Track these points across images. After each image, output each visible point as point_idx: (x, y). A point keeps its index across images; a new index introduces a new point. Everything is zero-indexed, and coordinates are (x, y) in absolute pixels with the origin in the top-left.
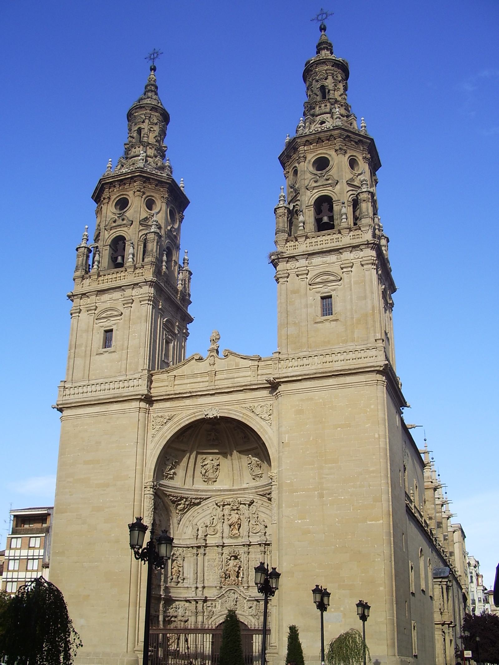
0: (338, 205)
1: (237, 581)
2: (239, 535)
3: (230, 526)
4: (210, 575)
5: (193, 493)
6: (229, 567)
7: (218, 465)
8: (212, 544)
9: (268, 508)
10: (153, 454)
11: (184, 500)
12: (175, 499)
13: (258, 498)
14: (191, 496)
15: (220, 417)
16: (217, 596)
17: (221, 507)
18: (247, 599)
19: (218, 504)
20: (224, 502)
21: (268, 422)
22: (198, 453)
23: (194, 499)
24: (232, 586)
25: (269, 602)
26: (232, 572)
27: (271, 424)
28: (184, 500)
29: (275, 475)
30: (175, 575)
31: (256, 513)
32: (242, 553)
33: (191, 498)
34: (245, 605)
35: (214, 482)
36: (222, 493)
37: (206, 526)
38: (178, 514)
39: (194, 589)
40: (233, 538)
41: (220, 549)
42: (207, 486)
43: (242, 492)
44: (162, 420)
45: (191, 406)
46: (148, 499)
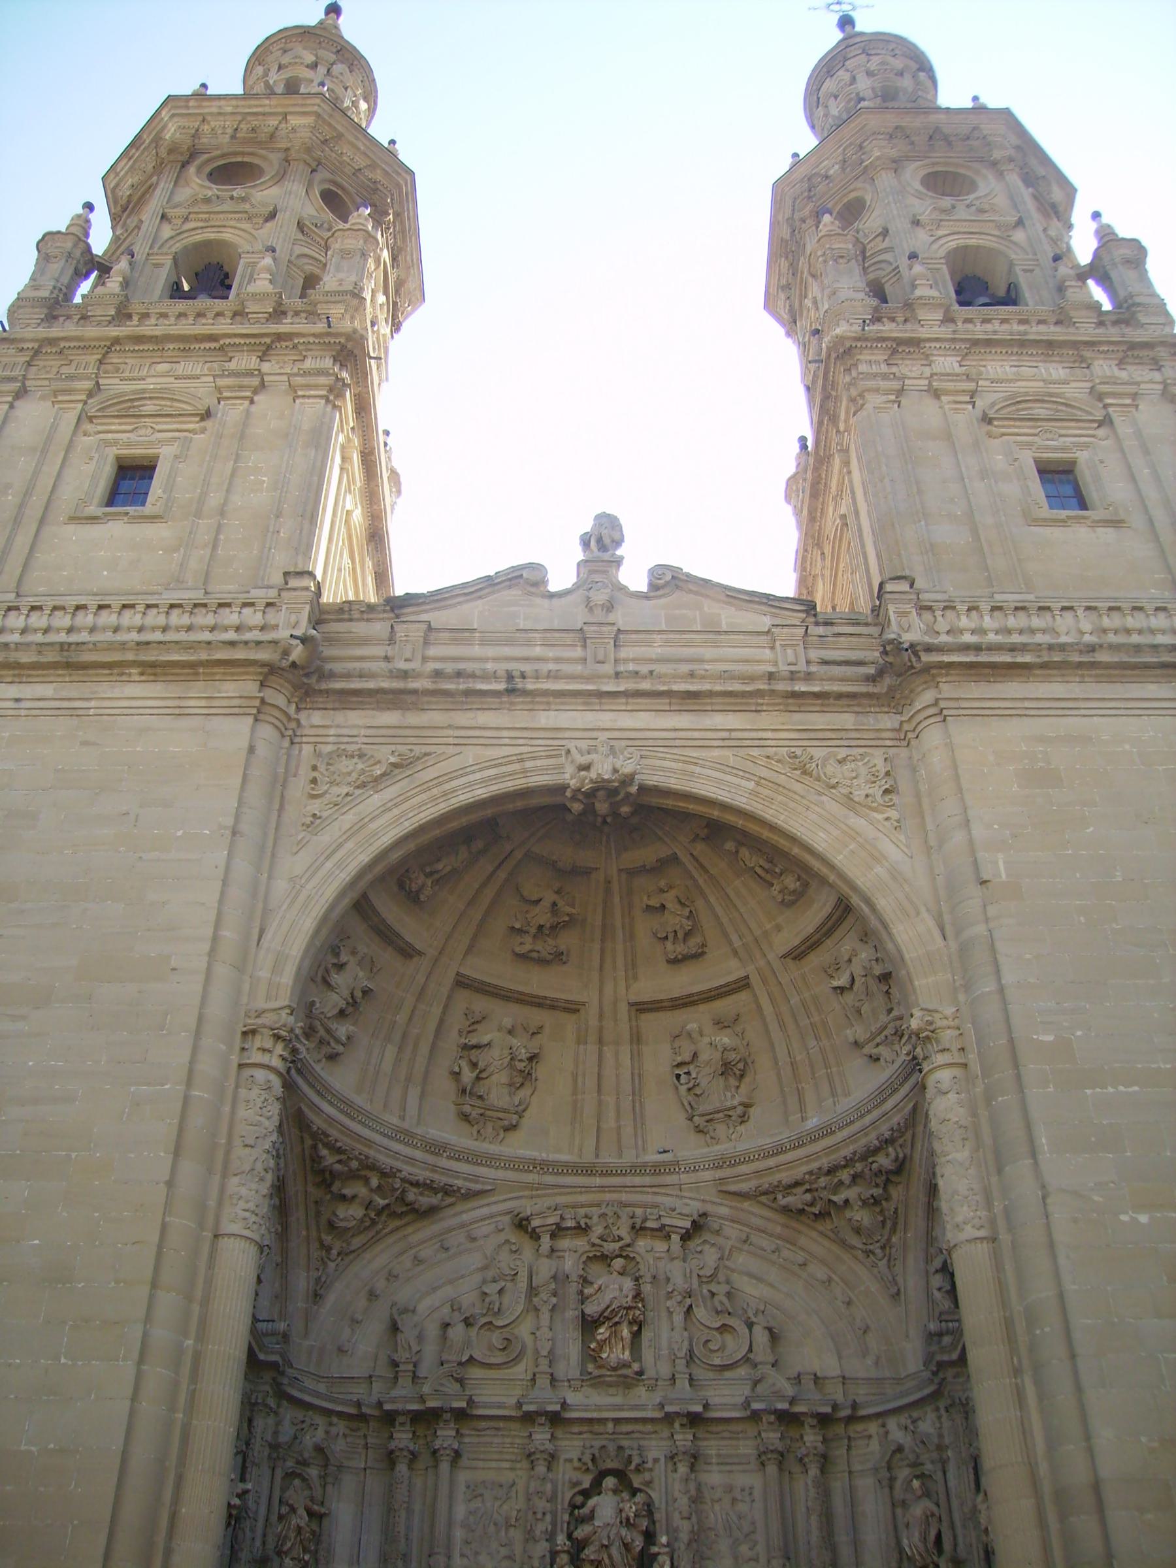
0: (1032, 271)
2: (640, 1373)
3: (589, 1325)
5: (418, 1154)
6: (597, 1523)
7: (531, 1059)
8: (500, 1406)
9: (774, 1257)
10: (302, 897)
11: (374, 1182)
12: (338, 1167)
13: (724, 1211)
14: (407, 1170)
15: (643, 789)
17: (546, 1240)
19: (535, 1223)
20: (562, 1218)
21: (880, 817)
23: (416, 1184)
27: (898, 821)
28: (374, 1182)
29: (945, 1022)
30: (294, 1554)
31: (721, 1277)
32: (656, 1461)
33: (403, 1180)
35: (507, 1129)
36: (549, 1179)
38: (328, 1249)
40: (610, 1385)
41: (541, 1435)
42: (476, 1143)
43: (647, 1180)
44: (360, 766)
45: (505, 733)
46: (255, 1092)
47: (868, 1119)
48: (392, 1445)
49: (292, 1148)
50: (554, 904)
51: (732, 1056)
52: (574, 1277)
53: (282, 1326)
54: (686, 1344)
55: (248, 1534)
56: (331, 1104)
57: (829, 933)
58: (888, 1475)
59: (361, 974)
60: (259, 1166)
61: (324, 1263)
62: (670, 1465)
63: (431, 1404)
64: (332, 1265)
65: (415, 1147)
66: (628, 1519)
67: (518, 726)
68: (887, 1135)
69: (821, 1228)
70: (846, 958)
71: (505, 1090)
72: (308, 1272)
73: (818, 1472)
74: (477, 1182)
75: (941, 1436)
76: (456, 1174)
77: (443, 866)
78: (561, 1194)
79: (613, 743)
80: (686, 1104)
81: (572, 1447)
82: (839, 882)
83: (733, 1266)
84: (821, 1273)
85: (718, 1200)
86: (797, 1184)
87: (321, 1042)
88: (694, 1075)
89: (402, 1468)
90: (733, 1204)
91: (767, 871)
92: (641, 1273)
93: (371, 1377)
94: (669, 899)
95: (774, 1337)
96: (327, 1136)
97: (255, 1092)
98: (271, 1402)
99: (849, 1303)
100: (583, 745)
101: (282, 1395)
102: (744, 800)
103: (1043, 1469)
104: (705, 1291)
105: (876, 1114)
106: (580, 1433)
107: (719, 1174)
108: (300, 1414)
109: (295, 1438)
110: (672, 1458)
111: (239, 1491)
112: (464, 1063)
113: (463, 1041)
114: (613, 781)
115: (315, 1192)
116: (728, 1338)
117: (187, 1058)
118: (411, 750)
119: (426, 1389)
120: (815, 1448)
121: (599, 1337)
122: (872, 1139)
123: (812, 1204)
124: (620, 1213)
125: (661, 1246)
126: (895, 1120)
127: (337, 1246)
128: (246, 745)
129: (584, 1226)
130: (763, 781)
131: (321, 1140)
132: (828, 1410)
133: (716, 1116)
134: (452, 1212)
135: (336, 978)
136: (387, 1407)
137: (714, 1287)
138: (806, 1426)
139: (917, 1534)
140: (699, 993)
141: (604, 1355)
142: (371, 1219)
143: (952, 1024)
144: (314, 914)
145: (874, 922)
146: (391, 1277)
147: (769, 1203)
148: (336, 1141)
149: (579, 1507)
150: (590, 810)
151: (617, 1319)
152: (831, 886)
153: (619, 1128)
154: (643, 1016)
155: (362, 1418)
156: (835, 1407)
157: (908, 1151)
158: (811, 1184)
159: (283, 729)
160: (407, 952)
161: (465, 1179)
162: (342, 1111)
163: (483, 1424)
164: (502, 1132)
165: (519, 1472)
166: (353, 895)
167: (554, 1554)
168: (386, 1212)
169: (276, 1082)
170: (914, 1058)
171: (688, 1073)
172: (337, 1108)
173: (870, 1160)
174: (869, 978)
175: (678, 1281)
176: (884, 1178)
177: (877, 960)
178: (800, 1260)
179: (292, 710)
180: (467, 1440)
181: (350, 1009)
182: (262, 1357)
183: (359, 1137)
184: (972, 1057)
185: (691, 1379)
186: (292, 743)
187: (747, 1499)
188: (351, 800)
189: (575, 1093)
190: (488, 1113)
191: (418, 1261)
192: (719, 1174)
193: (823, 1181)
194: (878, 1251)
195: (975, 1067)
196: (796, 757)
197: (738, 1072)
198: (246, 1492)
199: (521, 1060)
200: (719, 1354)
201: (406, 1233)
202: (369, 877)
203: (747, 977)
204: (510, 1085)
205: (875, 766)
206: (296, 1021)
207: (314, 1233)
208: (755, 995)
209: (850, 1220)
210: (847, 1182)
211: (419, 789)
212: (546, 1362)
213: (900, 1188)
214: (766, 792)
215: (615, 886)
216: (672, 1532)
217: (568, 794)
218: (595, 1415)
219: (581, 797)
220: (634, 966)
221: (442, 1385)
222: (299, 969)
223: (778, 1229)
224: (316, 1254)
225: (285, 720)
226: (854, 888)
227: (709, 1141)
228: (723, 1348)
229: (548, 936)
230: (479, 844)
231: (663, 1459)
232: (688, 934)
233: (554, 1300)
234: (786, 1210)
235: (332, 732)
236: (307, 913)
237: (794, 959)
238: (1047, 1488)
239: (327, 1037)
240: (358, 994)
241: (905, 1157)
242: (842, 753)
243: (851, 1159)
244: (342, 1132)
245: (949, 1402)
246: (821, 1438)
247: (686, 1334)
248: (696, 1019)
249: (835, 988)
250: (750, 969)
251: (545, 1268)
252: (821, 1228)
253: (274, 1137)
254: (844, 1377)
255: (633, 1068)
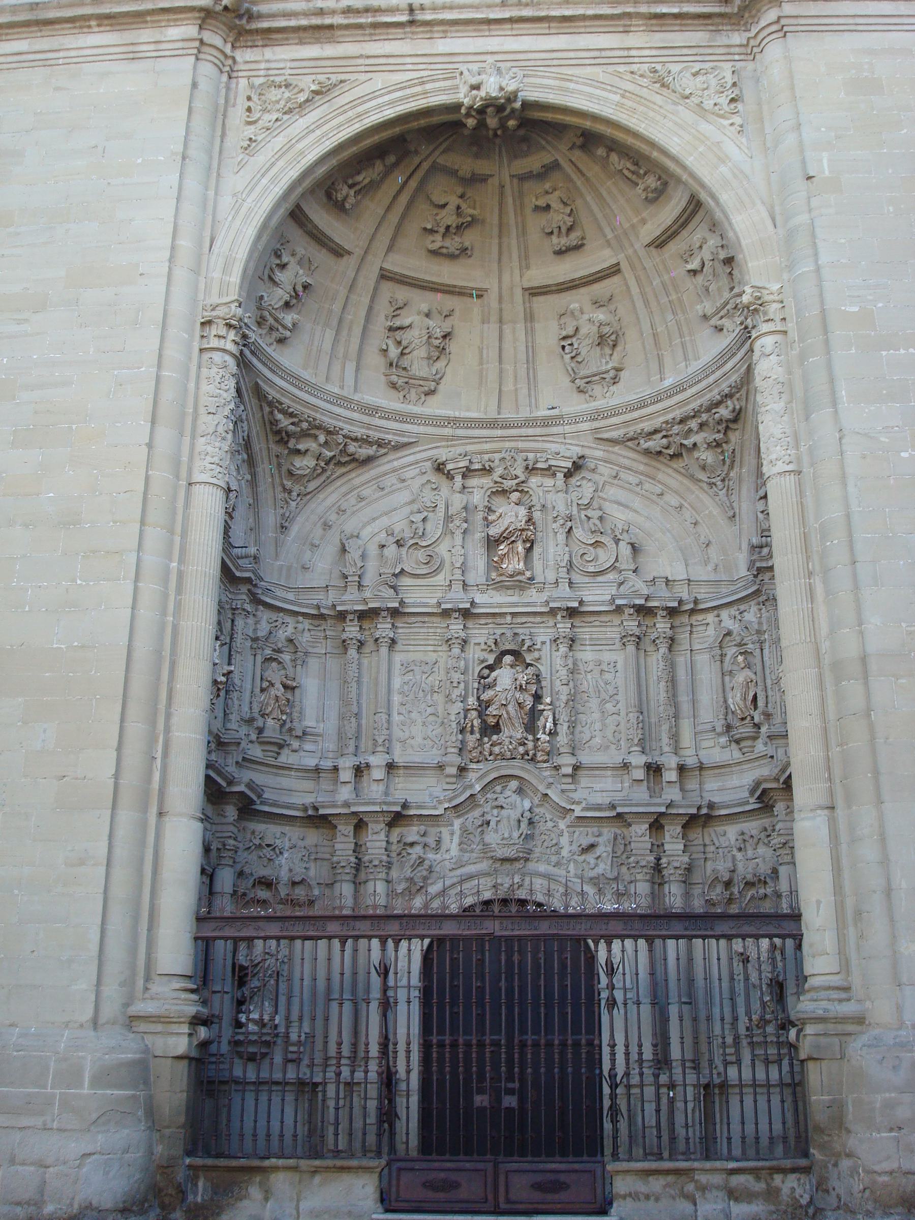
1: (530, 745)
3: (492, 543)
4: (413, 722)
5: (356, 416)
7: (444, 337)
8: (425, 605)
9: (638, 489)
11: (322, 438)
13: (599, 454)
14: (347, 428)
15: (526, 105)
16: (450, 800)
17: (458, 478)
18: (578, 812)
21: (726, 123)
22: (385, 276)
23: (356, 440)
24: (512, 763)
25: (666, 828)
26: (510, 708)
27: (741, 126)
31: (595, 504)
32: (543, 643)
34: (564, 841)
35: (427, 394)
36: (461, 432)
37: (397, 542)
39: (346, 775)
40: (508, 588)
41: (456, 627)
42: (403, 405)
43: (538, 431)
44: (287, 94)
45: (408, 60)
46: (215, 370)
47: (711, 379)
48: (344, 636)
49: (253, 414)
50: (458, 208)
51: (606, 330)
52: (481, 508)
53: (252, 550)
54: (567, 557)
55: (236, 702)
56: (282, 378)
57: (684, 225)
58: (719, 652)
59: (301, 272)
60: (221, 429)
61: (287, 502)
62: (554, 646)
63: (371, 605)
64: (293, 504)
65: (353, 410)
66: (521, 686)
67: (419, 53)
68: (727, 390)
69: (675, 466)
70: (697, 246)
71: (425, 363)
72: (275, 509)
73: (667, 651)
74: (404, 436)
75: (760, 623)
76: (387, 430)
77: (363, 178)
78: (470, 443)
79: (499, 64)
80: (570, 369)
81: (481, 634)
82: (690, 181)
83: (604, 496)
84: (674, 500)
85: (594, 445)
86: (656, 431)
87: (271, 329)
88: (576, 346)
89: (352, 652)
90: (606, 448)
91: (633, 173)
92: (532, 503)
93: (327, 586)
94: (553, 200)
95: (635, 549)
96: (281, 404)
97: (215, 370)
98: (248, 607)
99: (695, 524)
100: (475, 67)
101: (257, 601)
102: (611, 111)
103: (825, 646)
104: (583, 516)
105: (718, 374)
106: (486, 624)
107: (596, 424)
108: (274, 616)
109: (271, 633)
110: (555, 641)
111: (225, 672)
112: (390, 342)
113: (389, 324)
114: (500, 98)
115: (276, 449)
116: (600, 551)
117: (158, 346)
118: (329, 79)
119: (368, 594)
120: (665, 633)
121: (500, 553)
122: (715, 395)
123: (667, 448)
124: (516, 457)
125: (549, 482)
126: (734, 378)
127: (297, 489)
128: (189, 81)
129: (488, 468)
130: (627, 94)
131: (277, 407)
132: (675, 604)
133: (594, 378)
134: (386, 460)
135: (279, 276)
136: (339, 608)
137: (590, 513)
138: (658, 617)
139: (739, 695)
140: (580, 278)
141: (504, 566)
142: (323, 468)
143: (777, 298)
144: (254, 223)
145: (718, 215)
146: (341, 511)
147: (635, 447)
148: (289, 407)
149: (485, 678)
150: (482, 124)
151: (513, 539)
152: (685, 184)
153: (516, 390)
154: (535, 299)
155: (322, 617)
156: (681, 602)
157: (743, 404)
158: (667, 431)
159: (221, 66)
160: (338, 252)
161: (394, 434)
162: (292, 384)
163: (413, 619)
164: (423, 396)
165: (440, 654)
166: (288, 205)
167: (467, 711)
168: (333, 461)
169: (231, 362)
170: (746, 328)
171: (571, 345)
172: (287, 381)
173: (714, 411)
174: (716, 262)
175: (561, 508)
176: (724, 425)
177: (722, 246)
178: (659, 491)
179: (228, 49)
180: (400, 631)
181: (294, 301)
182: (238, 574)
183: (307, 404)
184: (791, 326)
185: (571, 583)
186: (230, 78)
187: (612, 670)
188: (280, 125)
189: (481, 364)
190: (411, 381)
191: (361, 499)
192: (596, 424)
193: (676, 429)
194: (719, 483)
195: (793, 334)
196: (656, 71)
197: (611, 343)
198: (230, 672)
199: (436, 338)
200: (593, 564)
201: (350, 477)
202: (299, 190)
203: (618, 264)
204: (429, 358)
205: (724, 78)
206: (245, 311)
207: (277, 480)
208: (625, 279)
209: (698, 459)
210: (695, 429)
211: (337, 112)
212: (460, 572)
213: (737, 433)
214: (629, 103)
215: (508, 190)
216: (554, 694)
217: (463, 111)
218: (497, 610)
219: (474, 113)
220: (527, 257)
221: (380, 591)
222: (245, 270)
223: (642, 468)
224: (280, 495)
225: (222, 58)
226: (703, 185)
227: (588, 398)
228: (596, 559)
229: (455, 234)
230: (391, 159)
231: (548, 643)
232: (570, 229)
233: (465, 525)
234: (647, 452)
235: (263, 66)
236: (248, 222)
237: (657, 247)
238: (827, 661)
239: (276, 325)
240: (299, 288)
241: (741, 409)
242: (697, 67)
243: (699, 411)
244: (294, 401)
245: (765, 597)
246: (669, 626)
247: (567, 549)
248: (576, 300)
249: (689, 271)
250: (621, 257)
251: (458, 501)
252: (675, 466)
253: (232, 406)
254: (689, 580)
255: (527, 342)
